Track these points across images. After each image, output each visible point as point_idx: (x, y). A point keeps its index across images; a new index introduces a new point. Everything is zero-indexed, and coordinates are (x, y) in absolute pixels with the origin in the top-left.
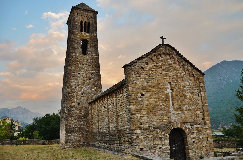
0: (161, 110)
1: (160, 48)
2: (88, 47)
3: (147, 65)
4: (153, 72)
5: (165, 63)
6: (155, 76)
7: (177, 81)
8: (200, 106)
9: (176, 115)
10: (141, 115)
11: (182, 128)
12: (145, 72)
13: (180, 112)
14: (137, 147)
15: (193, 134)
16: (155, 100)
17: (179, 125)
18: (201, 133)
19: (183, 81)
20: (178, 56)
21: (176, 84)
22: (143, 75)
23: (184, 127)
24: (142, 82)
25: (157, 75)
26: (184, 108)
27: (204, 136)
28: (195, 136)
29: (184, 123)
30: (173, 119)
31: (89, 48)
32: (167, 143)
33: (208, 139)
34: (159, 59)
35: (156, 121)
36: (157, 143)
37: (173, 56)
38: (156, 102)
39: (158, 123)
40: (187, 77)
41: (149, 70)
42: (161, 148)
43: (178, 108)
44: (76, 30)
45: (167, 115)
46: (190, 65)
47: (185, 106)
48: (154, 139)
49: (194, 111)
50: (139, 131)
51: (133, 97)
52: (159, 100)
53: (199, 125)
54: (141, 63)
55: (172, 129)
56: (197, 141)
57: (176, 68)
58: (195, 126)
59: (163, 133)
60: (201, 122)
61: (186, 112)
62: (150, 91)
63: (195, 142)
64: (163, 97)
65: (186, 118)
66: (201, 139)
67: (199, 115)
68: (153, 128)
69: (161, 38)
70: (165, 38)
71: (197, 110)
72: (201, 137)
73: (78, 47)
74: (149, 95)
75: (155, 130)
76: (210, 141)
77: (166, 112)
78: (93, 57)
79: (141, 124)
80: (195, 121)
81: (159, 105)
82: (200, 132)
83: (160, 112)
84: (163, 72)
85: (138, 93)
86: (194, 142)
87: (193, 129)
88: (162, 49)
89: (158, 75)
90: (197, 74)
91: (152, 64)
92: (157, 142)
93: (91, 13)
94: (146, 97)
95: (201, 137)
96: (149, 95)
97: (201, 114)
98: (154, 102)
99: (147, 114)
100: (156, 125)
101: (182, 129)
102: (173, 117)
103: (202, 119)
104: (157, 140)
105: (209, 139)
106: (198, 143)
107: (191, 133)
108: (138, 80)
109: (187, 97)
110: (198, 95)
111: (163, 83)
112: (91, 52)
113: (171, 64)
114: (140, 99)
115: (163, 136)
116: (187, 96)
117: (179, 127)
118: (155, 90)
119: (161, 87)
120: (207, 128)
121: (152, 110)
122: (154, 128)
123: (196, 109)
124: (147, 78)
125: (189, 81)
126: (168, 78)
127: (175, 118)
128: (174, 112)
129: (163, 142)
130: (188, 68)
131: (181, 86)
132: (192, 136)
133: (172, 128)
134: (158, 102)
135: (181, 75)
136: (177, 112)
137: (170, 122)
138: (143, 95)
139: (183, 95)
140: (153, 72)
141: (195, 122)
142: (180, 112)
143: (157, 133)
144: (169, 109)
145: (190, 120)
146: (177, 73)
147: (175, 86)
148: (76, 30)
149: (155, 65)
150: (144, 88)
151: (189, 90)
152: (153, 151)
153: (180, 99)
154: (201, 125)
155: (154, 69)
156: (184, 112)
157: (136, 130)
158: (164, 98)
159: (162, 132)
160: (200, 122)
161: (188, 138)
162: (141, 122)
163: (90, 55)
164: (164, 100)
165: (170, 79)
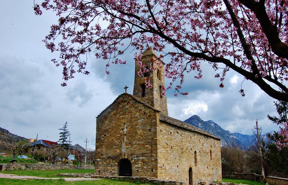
0: (115, 145)
1: (120, 98)
2: (146, 89)
3: (110, 114)
4: (113, 118)
5: (122, 109)
6: (114, 120)
7: (131, 122)
8: (150, 140)
9: (126, 148)
10: (103, 149)
11: (128, 159)
12: (108, 119)
13: (130, 146)
14: (97, 169)
15: (137, 165)
16: (112, 138)
17: (126, 156)
18: (146, 164)
19: (136, 120)
20: (133, 100)
21: (130, 124)
22: (107, 122)
23: (130, 158)
24: (105, 127)
25: (116, 120)
26: (134, 143)
27: (149, 167)
28: (140, 166)
29: (132, 155)
30: (124, 152)
31: (147, 91)
32: (116, 169)
33: (152, 171)
34: (119, 106)
35: (111, 153)
36: (108, 168)
37: (129, 102)
38: (113, 140)
39: (112, 154)
40: (140, 116)
41: (111, 117)
42: (111, 172)
43: (129, 143)
44: (137, 77)
45: (119, 149)
46: (143, 105)
47: (135, 141)
48: (107, 165)
49: (144, 145)
50: (99, 160)
51: (98, 138)
52: (115, 138)
53: (145, 157)
54: (105, 114)
55: (121, 160)
56: (141, 170)
57: (131, 111)
58: (141, 158)
59: (113, 162)
60: (149, 154)
61: (135, 146)
62: (110, 132)
63: (139, 171)
64: (118, 135)
65: (134, 151)
66: (146, 169)
67: (148, 148)
68: (107, 158)
69: (124, 88)
70: (127, 88)
71: (146, 144)
72: (145, 167)
73: (138, 92)
74: (109, 135)
75: (109, 159)
76: (155, 172)
77: (119, 147)
78: (149, 97)
79: (102, 155)
80: (143, 153)
81: (114, 141)
82: (144, 163)
83: (114, 147)
84: (121, 117)
85: (101, 135)
86: (138, 171)
87: (138, 160)
88: (121, 98)
89: (117, 120)
90: (149, 112)
91: (113, 112)
92: (109, 168)
93: (149, 57)
94: (107, 137)
95: (145, 167)
96: (109, 135)
97: (150, 147)
98: (112, 140)
99: (106, 148)
100: (111, 156)
101: (128, 160)
102: (123, 150)
103: (150, 151)
104: (109, 166)
105: (154, 170)
106: (142, 172)
107: (136, 162)
108: (103, 126)
109: (138, 134)
110: (150, 130)
111: (120, 125)
112: (147, 93)
113: (127, 109)
114: (103, 139)
115: (113, 164)
116: (137, 133)
117: (126, 158)
118: (113, 131)
119: (117, 128)
120: (153, 160)
121: (109, 146)
122: (108, 158)
123: (145, 144)
124: (109, 123)
125: (142, 119)
126: (124, 120)
127: (125, 150)
128: (125, 147)
129: (113, 168)
130: (141, 108)
131: (133, 125)
132: (136, 166)
133: (121, 159)
134: (114, 140)
135: (135, 116)
136: (128, 147)
137: (121, 154)
138: (105, 135)
139: (134, 132)
140: (113, 118)
141: (143, 155)
142: (130, 146)
143: (110, 162)
144: (121, 144)
145: (138, 152)
146: (131, 115)
147: (128, 126)
148: (137, 78)
149: (115, 113)
150: (106, 131)
151: (141, 128)
152: (106, 173)
153: (131, 136)
154: (147, 157)
155: (114, 115)
156: (133, 146)
157: (97, 159)
158: (118, 136)
159: (112, 161)
160: (148, 155)
161: (132, 167)
162: (102, 154)
163: (146, 97)
164: (118, 138)
165: (125, 121)
